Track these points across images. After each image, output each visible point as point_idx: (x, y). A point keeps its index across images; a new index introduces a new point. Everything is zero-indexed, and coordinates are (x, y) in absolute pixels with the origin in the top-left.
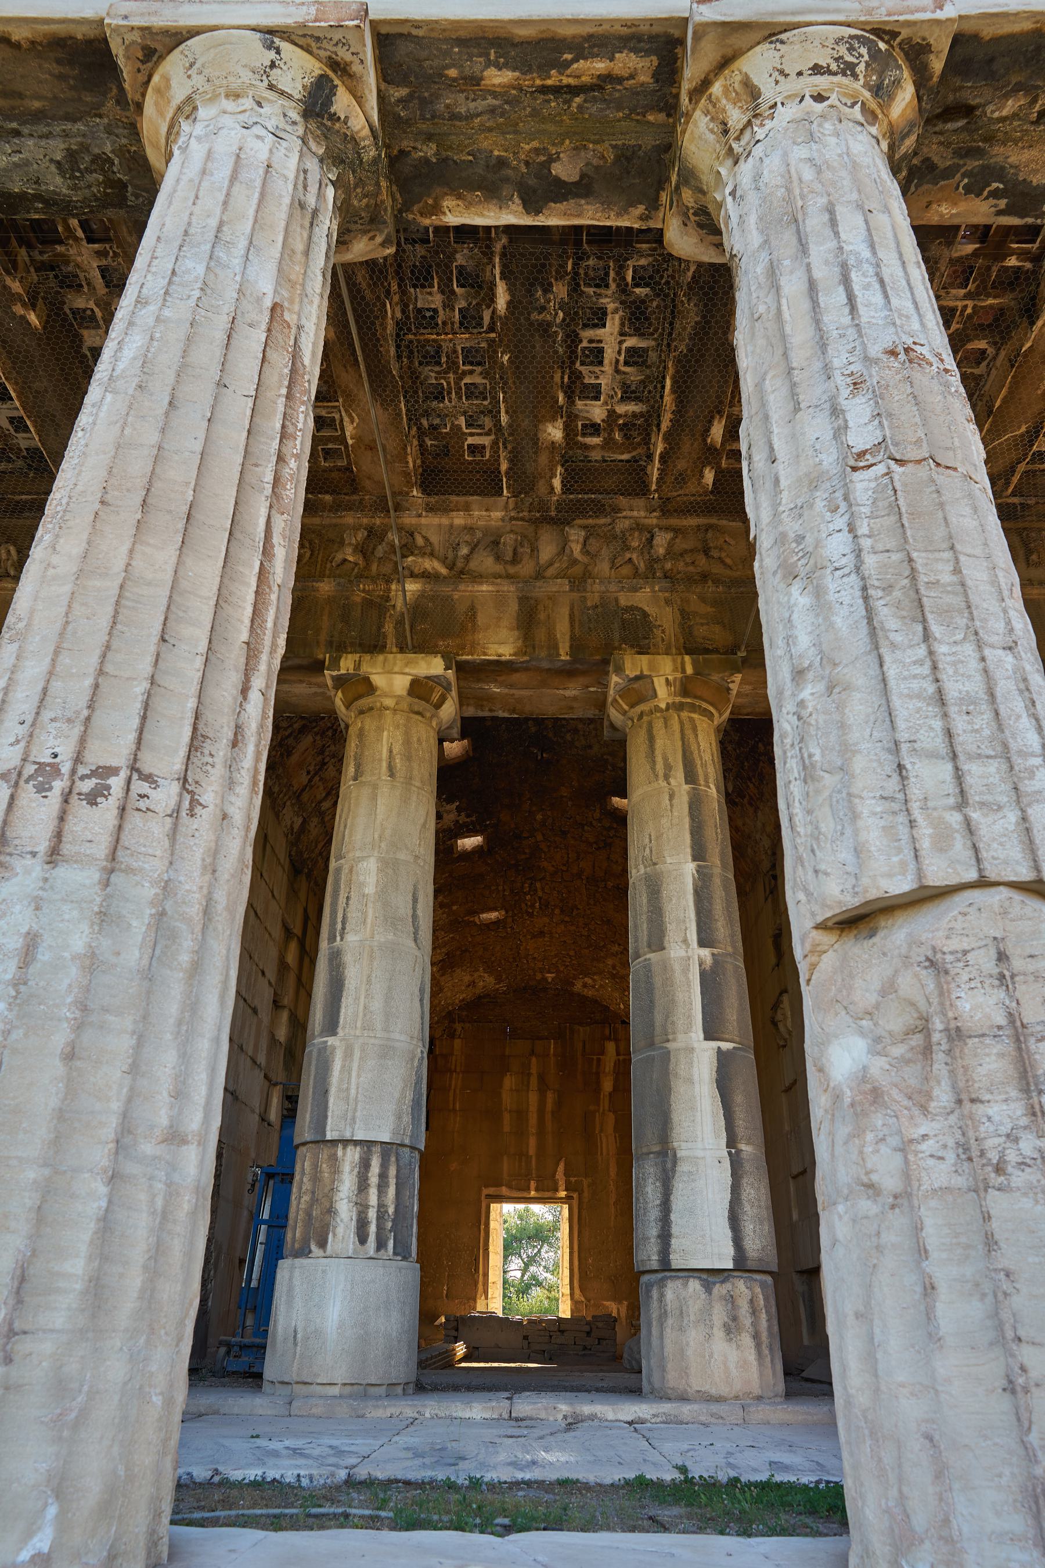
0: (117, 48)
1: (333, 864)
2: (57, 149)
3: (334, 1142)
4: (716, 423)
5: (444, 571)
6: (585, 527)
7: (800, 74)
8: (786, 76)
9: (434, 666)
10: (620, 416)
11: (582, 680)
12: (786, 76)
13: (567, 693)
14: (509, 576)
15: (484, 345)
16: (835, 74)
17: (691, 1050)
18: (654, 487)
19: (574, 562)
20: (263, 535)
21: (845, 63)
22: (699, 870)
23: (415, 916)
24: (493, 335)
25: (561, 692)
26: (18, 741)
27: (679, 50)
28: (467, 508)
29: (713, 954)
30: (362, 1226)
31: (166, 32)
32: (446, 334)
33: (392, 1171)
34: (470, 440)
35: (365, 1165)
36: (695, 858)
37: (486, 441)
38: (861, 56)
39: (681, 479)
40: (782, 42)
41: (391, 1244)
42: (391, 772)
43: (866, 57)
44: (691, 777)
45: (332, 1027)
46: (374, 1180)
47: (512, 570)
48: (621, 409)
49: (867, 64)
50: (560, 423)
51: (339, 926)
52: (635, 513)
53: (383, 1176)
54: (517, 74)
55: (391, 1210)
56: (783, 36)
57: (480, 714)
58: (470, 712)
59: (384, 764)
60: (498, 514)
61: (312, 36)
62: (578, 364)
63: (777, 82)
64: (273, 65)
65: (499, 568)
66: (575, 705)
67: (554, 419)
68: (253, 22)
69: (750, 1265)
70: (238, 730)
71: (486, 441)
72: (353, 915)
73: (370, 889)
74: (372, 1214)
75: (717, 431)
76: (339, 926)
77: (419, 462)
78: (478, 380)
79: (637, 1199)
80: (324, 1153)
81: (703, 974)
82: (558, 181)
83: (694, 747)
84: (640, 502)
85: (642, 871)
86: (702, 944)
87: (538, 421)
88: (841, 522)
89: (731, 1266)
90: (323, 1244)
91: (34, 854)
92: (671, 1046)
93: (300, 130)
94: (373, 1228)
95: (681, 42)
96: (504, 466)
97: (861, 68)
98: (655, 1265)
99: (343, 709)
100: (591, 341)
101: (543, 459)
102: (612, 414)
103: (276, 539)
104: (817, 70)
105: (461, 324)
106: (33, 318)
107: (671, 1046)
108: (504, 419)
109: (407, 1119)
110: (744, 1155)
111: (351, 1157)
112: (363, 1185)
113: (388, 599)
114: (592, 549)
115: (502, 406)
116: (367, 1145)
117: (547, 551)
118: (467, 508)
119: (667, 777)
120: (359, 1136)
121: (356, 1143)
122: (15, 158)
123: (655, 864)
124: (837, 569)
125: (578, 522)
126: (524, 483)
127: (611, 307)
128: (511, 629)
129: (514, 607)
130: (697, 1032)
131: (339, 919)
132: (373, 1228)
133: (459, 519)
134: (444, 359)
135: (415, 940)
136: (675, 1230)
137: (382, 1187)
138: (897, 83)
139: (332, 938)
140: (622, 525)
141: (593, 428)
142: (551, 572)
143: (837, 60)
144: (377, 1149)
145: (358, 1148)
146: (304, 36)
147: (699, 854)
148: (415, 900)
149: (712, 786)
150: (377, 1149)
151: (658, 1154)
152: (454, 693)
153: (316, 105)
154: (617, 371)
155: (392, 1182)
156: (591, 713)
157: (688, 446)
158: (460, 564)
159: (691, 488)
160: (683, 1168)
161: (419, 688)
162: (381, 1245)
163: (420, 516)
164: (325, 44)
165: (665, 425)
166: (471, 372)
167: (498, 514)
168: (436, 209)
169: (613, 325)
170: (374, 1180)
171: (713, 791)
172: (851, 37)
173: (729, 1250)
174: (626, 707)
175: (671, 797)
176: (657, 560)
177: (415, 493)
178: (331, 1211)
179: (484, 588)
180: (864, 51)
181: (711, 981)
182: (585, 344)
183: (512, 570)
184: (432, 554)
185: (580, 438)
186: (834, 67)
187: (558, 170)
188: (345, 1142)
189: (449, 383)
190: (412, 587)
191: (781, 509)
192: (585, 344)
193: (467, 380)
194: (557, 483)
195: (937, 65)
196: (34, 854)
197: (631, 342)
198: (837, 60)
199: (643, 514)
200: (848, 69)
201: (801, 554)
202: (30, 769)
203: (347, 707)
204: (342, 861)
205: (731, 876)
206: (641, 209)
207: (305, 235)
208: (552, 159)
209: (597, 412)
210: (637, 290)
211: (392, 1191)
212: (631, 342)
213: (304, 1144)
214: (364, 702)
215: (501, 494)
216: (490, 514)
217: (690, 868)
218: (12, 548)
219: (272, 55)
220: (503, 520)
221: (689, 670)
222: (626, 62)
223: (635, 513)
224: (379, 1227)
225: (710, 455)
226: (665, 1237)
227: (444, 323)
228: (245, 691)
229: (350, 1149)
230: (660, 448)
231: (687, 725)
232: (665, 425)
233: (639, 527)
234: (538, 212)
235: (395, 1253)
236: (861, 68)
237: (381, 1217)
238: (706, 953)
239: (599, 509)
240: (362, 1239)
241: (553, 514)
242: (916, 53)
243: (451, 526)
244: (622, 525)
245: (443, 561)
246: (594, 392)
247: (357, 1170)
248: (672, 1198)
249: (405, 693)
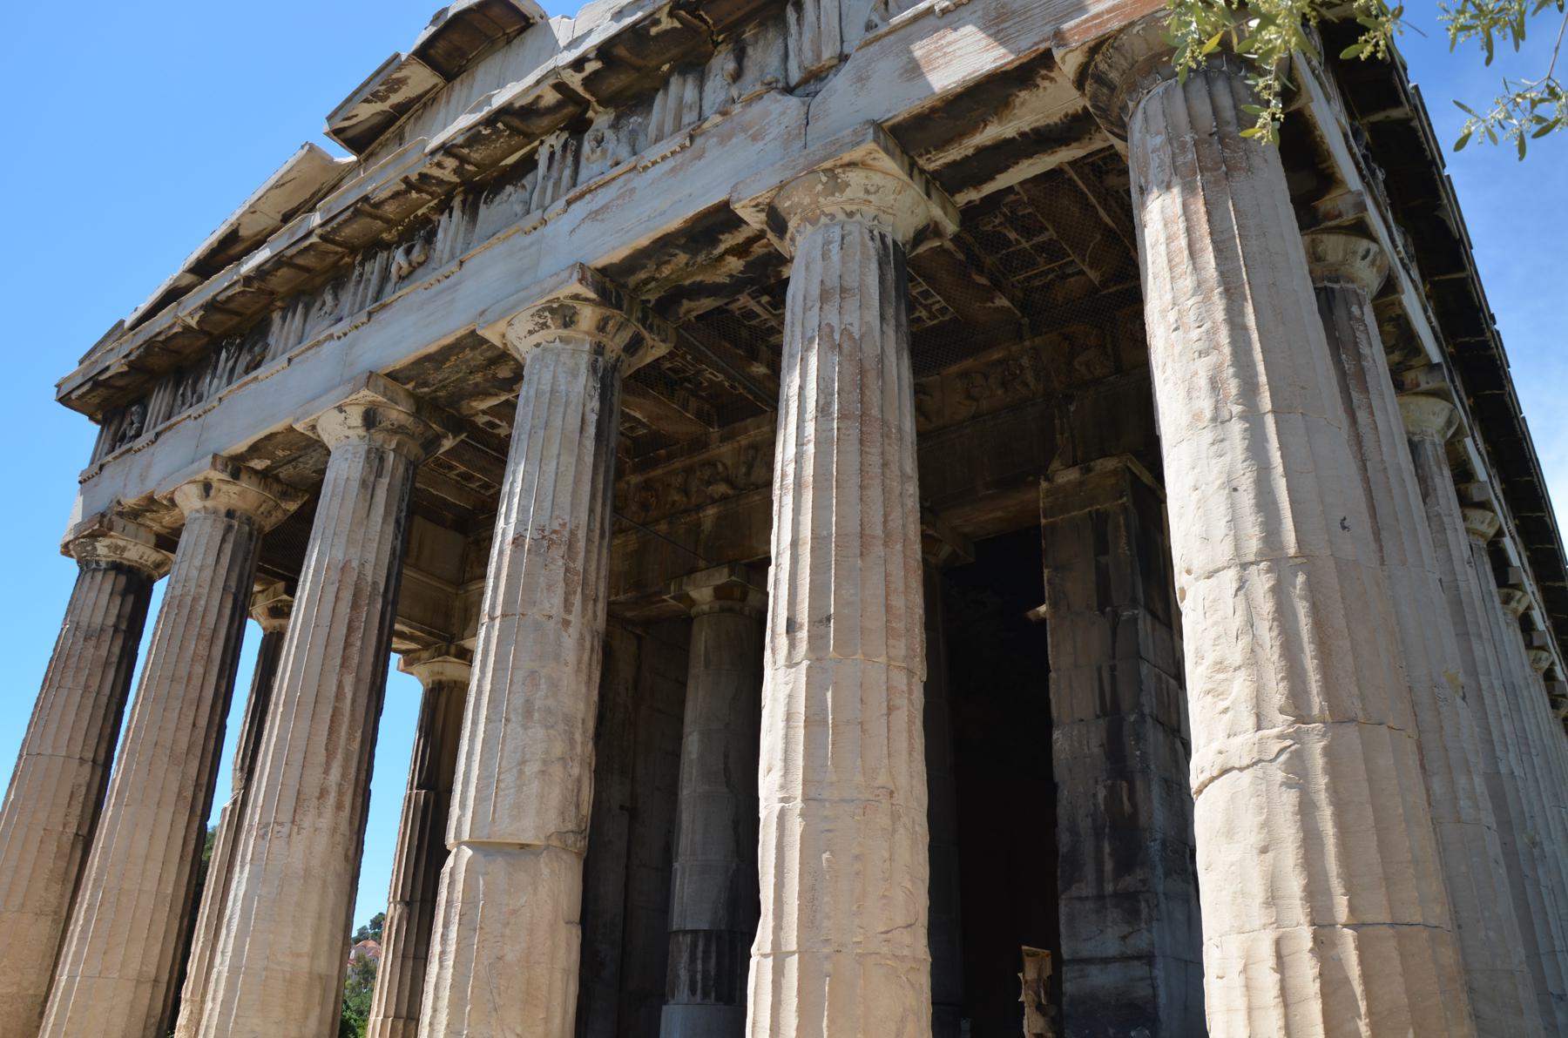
33: (714, 948)
53: (706, 952)
73: (694, 756)
74: (699, 976)
82: (505, 379)
97: (550, 322)
104: (530, 332)
112: (693, 959)
116: (695, 932)
137: (705, 960)
161: (719, 592)
162: (705, 995)
170: (700, 955)
188: (685, 932)
190: (711, 511)
200: (544, 326)
211: (713, 962)
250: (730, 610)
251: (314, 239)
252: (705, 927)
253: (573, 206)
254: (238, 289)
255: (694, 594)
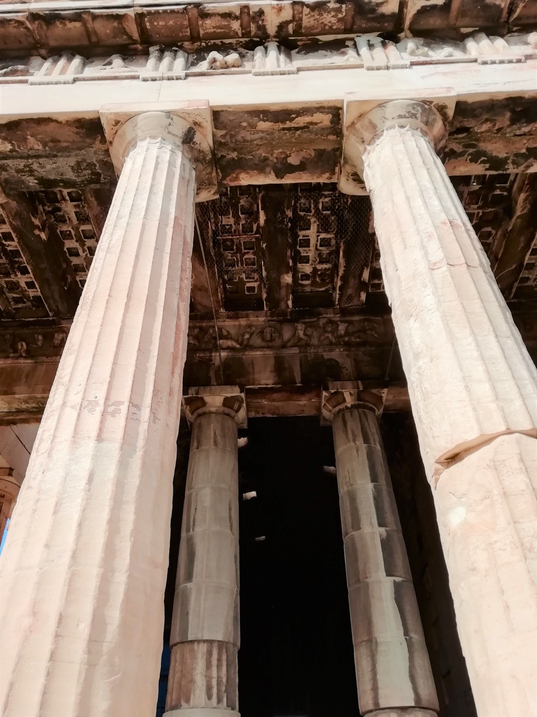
0: (103, 122)
1: (187, 493)
2: (72, 161)
3: (192, 642)
4: (365, 270)
5: (238, 346)
6: (304, 323)
7: (393, 118)
8: (387, 119)
9: (234, 392)
10: (319, 270)
11: (308, 396)
12: (387, 119)
13: (301, 403)
14: (268, 347)
15: (254, 240)
16: (408, 118)
17: (380, 582)
18: (337, 303)
19: (300, 339)
20: (176, 309)
21: (412, 113)
22: (375, 487)
23: (230, 517)
24: (258, 235)
25: (298, 402)
26: (78, 393)
27: (340, 111)
28: (247, 316)
29: (386, 531)
30: (209, 689)
31: (125, 114)
32: (236, 236)
33: (224, 657)
34: (248, 285)
35: (210, 653)
36: (373, 481)
37: (255, 285)
38: (418, 110)
39: (350, 298)
40: (384, 107)
41: (225, 699)
42: (216, 444)
43: (421, 111)
44: (366, 440)
45: (189, 577)
46: (214, 662)
47: (270, 344)
48: (319, 267)
49: (421, 114)
50: (290, 274)
51: (192, 524)
52: (328, 316)
53: (219, 660)
54: (272, 123)
55: (224, 680)
56: (384, 105)
57: (258, 416)
58: (253, 414)
59: (212, 440)
60: (262, 319)
61: (186, 113)
62: (298, 247)
63: (384, 122)
64: (170, 124)
65: (264, 344)
66: (305, 409)
67: (287, 273)
68: (162, 109)
69: (424, 704)
70: (171, 390)
71: (255, 285)
72: (199, 517)
74: (214, 682)
75: (366, 275)
76: (192, 524)
77: (223, 296)
78: (252, 256)
79: (358, 670)
80: (187, 647)
81: (382, 541)
82: (290, 165)
83: (366, 424)
84: (331, 310)
85: (346, 489)
86: (380, 525)
87: (280, 274)
88: (429, 291)
89: (412, 704)
90: (188, 701)
91: (89, 438)
92: (368, 580)
93: (181, 149)
94: (215, 691)
95: (341, 108)
96: (264, 296)
97: (419, 115)
98: (371, 707)
99: (190, 415)
100: (304, 236)
101: (283, 292)
102: (315, 270)
103: (181, 312)
104: (400, 117)
105: (243, 231)
106: (43, 236)
107: (368, 580)
108: (264, 274)
109: (231, 627)
110: (414, 640)
111: (202, 648)
112: (209, 665)
113: (211, 360)
114: (309, 333)
115: (263, 268)
116: (210, 642)
117: (287, 334)
118: (247, 316)
119: (354, 441)
120: (206, 638)
121: (205, 641)
122: (54, 166)
123: (352, 485)
124: (429, 310)
125: (302, 320)
126: (274, 303)
127: (312, 220)
128: (272, 372)
129: (272, 362)
130: (382, 572)
131: (192, 520)
132: (215, 691)
133: (243, 322)
134: (235, 247)
135: (231, 530)
136: (380, 684)
137: (219, 667)
138: (434, 120)
139: (188, 530)
140: (322, 322)
141: (306, 277)
142: (290, 344)
143: (408, 112)
144: (215, 645)
145: (206, 644)
146: (183, 113)
147: (374, 479)
148: (230, 509)
149: (378, 445)
150: (215, 645)
151: (368, 641)
152: (244, 405)
153: (188, 139)
154: (316, 249)
155: (224, 663)
156: (313, 413)
157: (352, 282)
158: (245, 342)
159: (355, 302)
160: (381, 648)
161: (228, 402)
162: (219, 701)
163: (225, 321)
164: (191, 116)
165: (341, 272)
166: (248, 253)
167: (262, 319)
168: (237, 178)
169: (314, 228)
170: (214, 662)
171: (378, 447)
172: (413, 104)
173: (412, 695)
174: (331, 408)
175: (357, 450)
176: (341, 336)
177: (222, 310)
178: (192, 681)
179: (258, 353)
180: (419, 109)
181: (386, 545)
182: (301, 238)
183: (270, 344)
184: (231, 339)
185: (300, 282)
186: (407, 115)
187: (290, 160)
188: (199, 641)
189: (237, 258)
191: (402, 289)
192: (301, 238)
193: (246, 257)
194: (290, 303)
195: (451, 112)
196: (89, 438)
197: (323, 236)
198: (408, 112)
199: (332, 315)
201: (413, 306)
202: (86, 403)
203: (192, 413)
204: (192, 490)
205: (392, 490)
206: (327, 175)
207: (185, 189)
208: (287, 156)
209: (307, 269)
210: (325, 212)
212: (323, 236)
213: (175, 645)
214: (200, 411)
215: (263, 309)
216: (259, 319)
217: (370, 486)
218: (24, 344)
219: (170, 120)
220: (264, 321)
221: (361, 388)
222: (318, 117)
223: (328, 316)
224: (219, 690)
225: (363, 286)
226: (375, 689)
227: (235, 231)
228: (173, 373)
229: (201, 644)
230: (339, 283)
231: (362, 415)
232: (341, 272)
233: (330, 322)
234: (282, 178)
235: (228, 706)
236: (419, 115)
237: (219, 683)
238: (382, 530)
239: (312, 314)
240: (210, 697)
241: (289, 317)
242: (442, 109)
243: (240, 325)
244: (322, 322)
245: (237, 341)
246: (306, 260)
247: (205, 657)
248: (377, 666)
249: (221, 405)
250: (228, 415)
251: (131, 12)
252: (220, 637)
253: (415, 67)
254: (20, 17)
255: (208, 399)
